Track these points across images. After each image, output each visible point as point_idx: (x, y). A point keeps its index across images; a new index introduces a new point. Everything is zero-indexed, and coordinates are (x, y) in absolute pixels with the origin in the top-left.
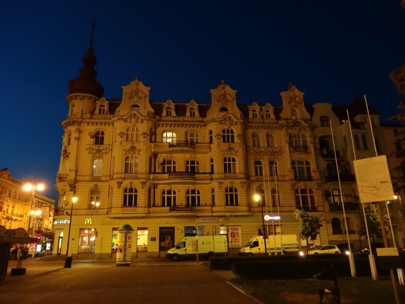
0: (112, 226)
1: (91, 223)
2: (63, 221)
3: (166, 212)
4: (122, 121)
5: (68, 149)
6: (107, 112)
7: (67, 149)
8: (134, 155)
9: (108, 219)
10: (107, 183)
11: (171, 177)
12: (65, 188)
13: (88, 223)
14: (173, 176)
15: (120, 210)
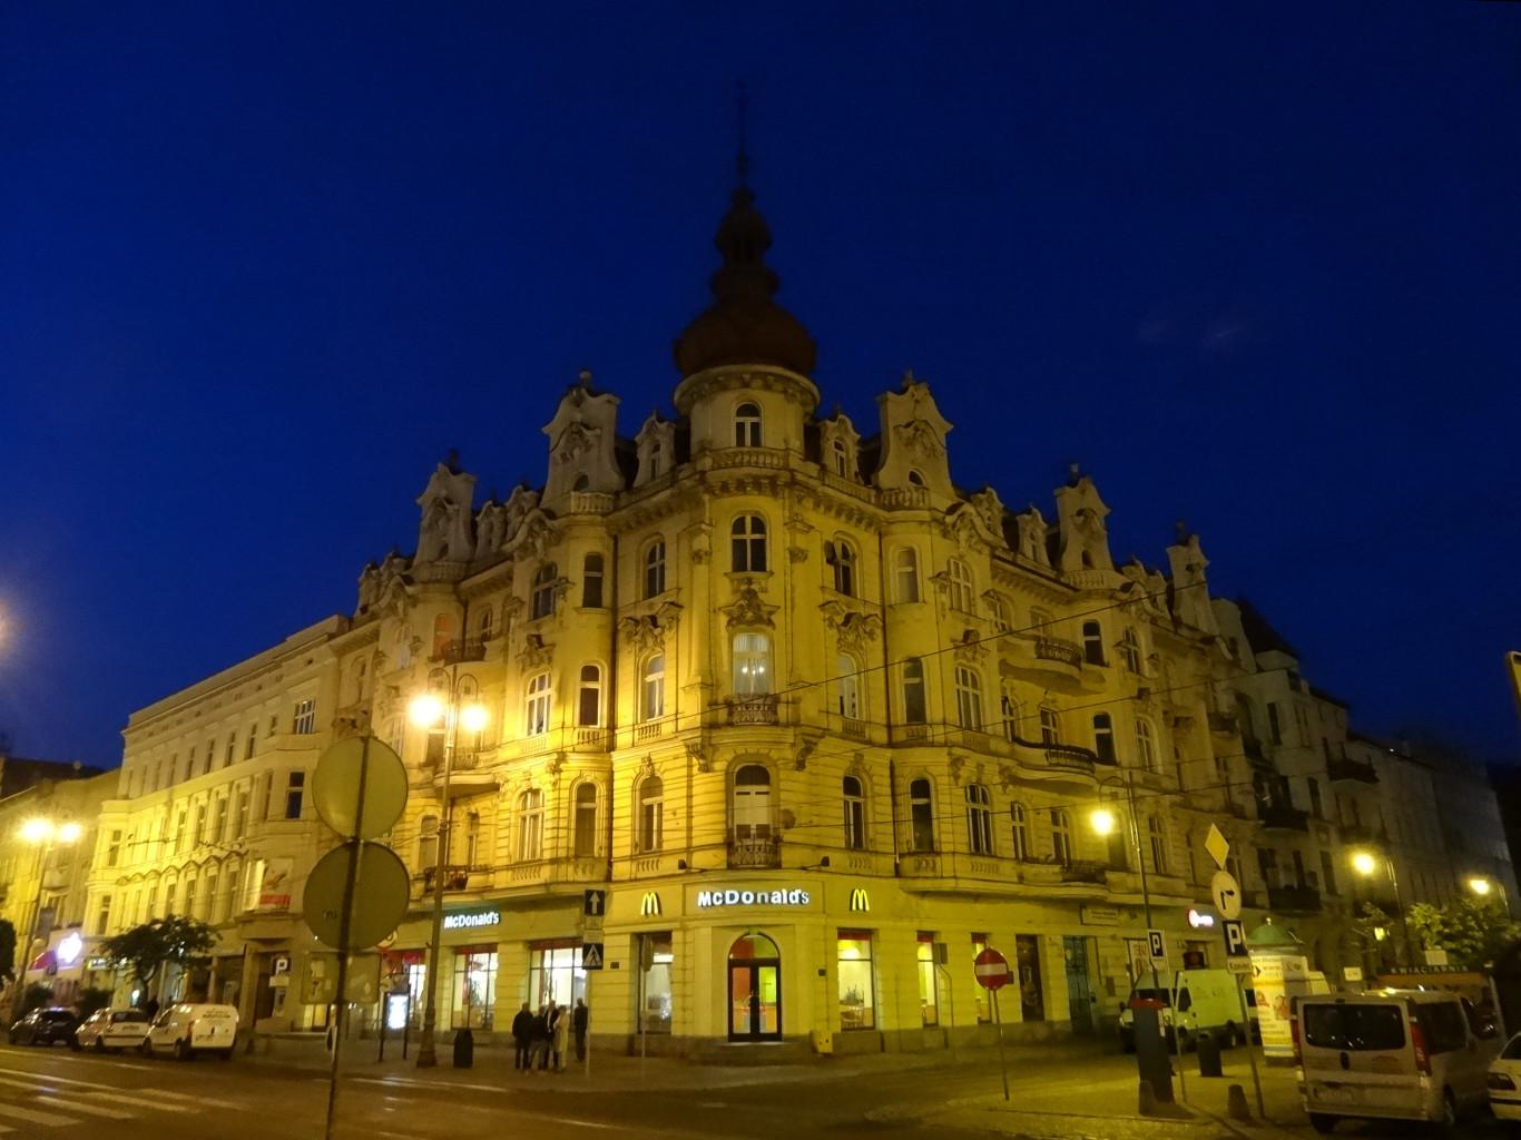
0: (916, 925)
1: (867, 908)
2: (785, 892)
3: (1052, 882)
4: (936, 531)
5: (764, 591)
6: (856, 474)
7: (753, 587)
8: (973, 664)
9: (902, 896)
10: (889, 753)
11: (1054, 760)
12: (774, 755)
13: (861, 907)
14: (1062, 761)
15: (963, 865)
